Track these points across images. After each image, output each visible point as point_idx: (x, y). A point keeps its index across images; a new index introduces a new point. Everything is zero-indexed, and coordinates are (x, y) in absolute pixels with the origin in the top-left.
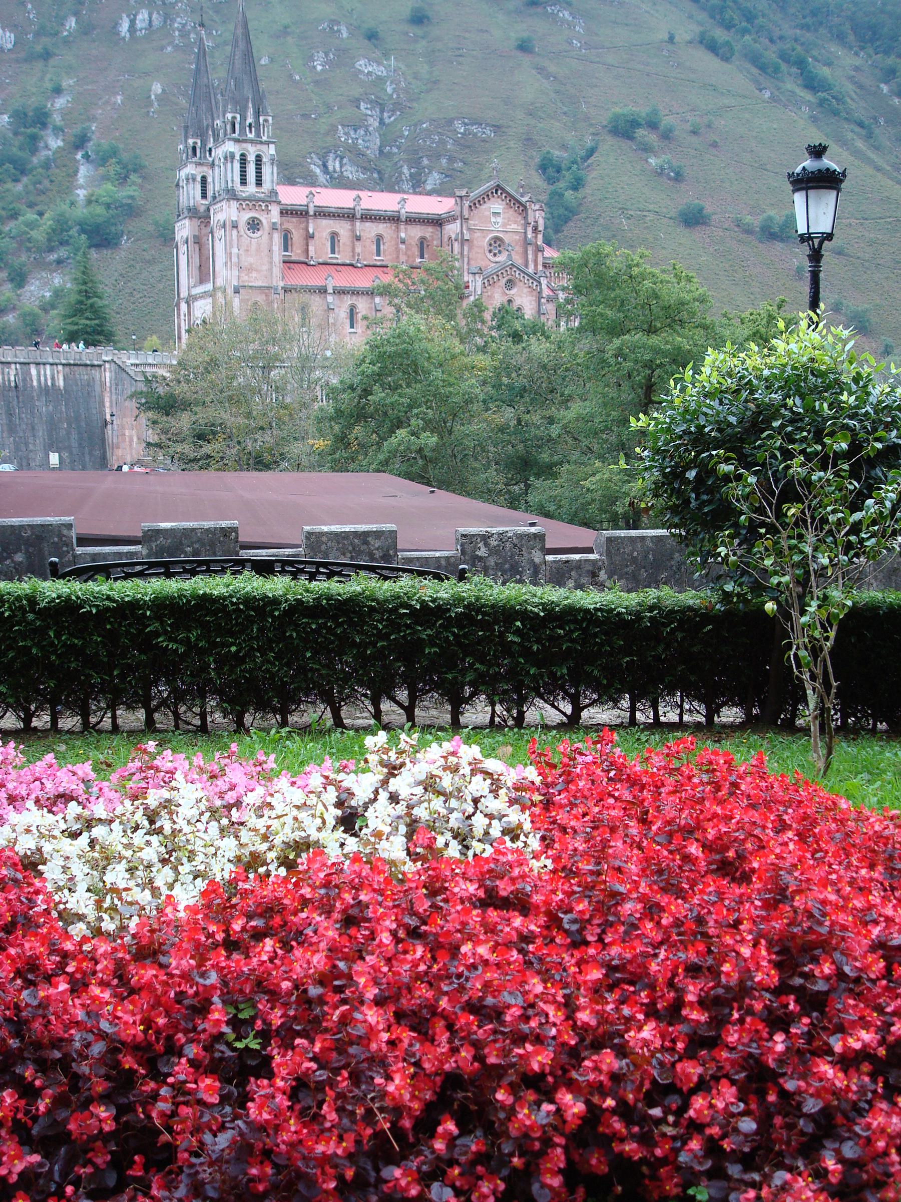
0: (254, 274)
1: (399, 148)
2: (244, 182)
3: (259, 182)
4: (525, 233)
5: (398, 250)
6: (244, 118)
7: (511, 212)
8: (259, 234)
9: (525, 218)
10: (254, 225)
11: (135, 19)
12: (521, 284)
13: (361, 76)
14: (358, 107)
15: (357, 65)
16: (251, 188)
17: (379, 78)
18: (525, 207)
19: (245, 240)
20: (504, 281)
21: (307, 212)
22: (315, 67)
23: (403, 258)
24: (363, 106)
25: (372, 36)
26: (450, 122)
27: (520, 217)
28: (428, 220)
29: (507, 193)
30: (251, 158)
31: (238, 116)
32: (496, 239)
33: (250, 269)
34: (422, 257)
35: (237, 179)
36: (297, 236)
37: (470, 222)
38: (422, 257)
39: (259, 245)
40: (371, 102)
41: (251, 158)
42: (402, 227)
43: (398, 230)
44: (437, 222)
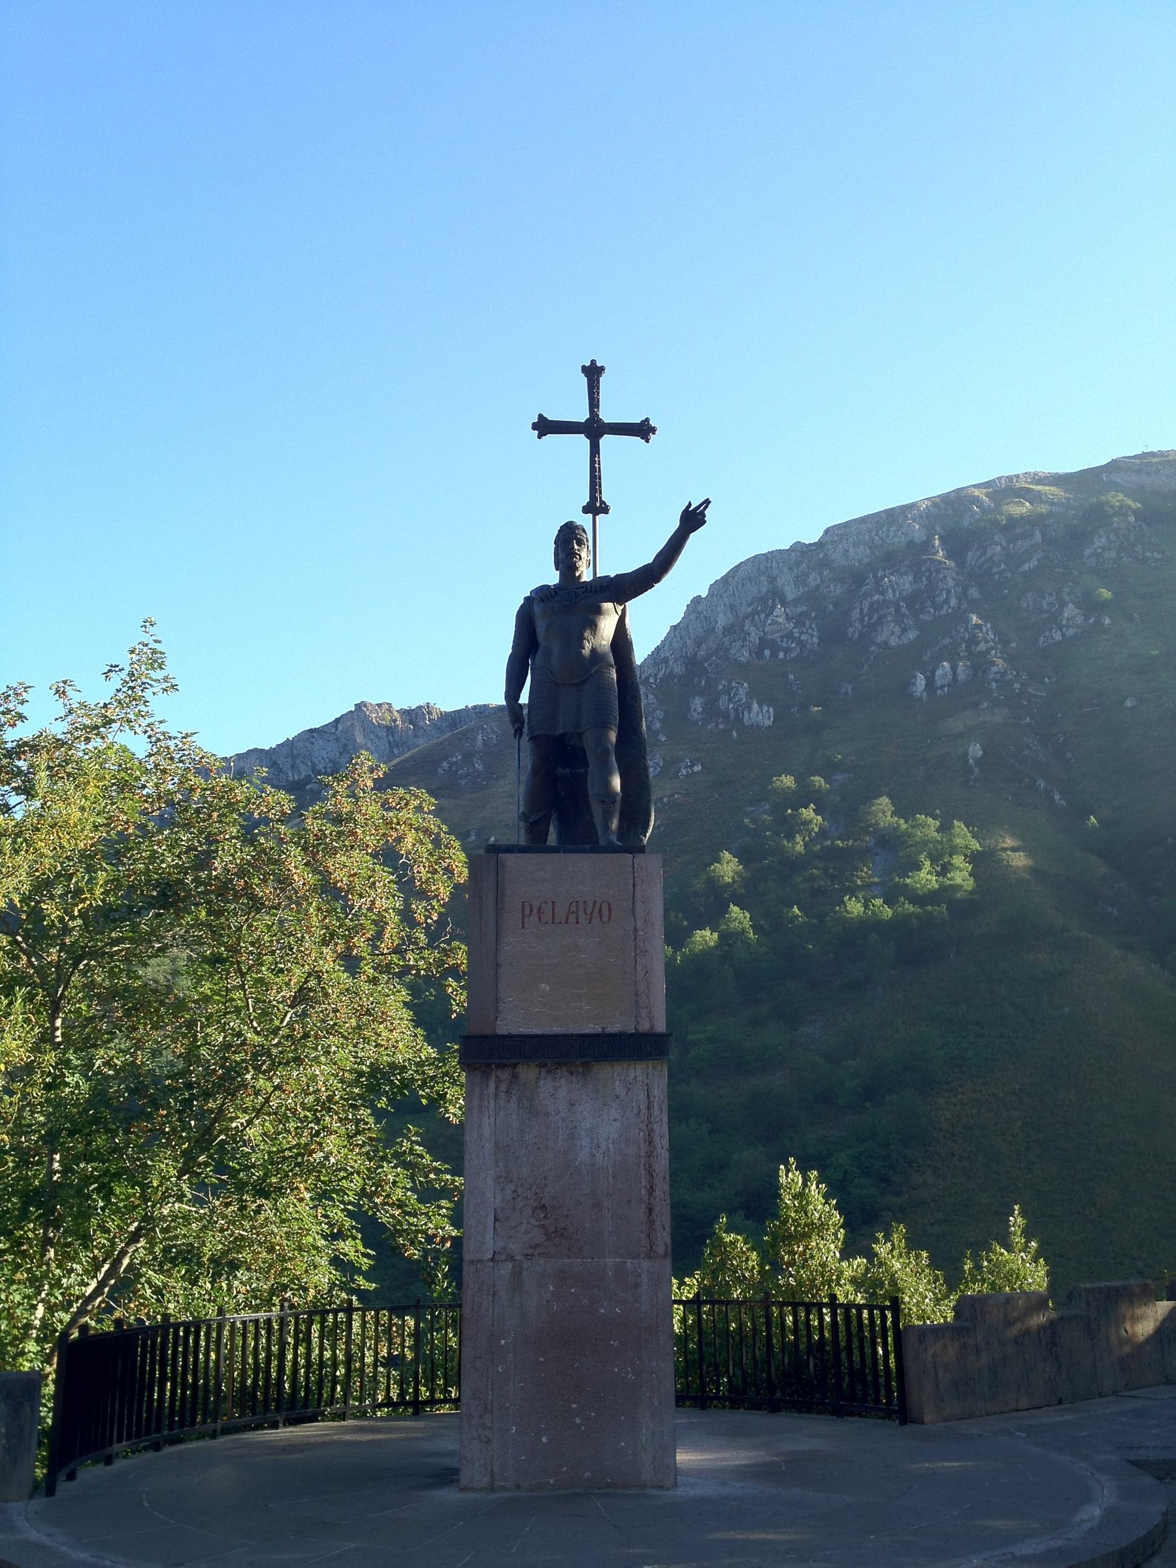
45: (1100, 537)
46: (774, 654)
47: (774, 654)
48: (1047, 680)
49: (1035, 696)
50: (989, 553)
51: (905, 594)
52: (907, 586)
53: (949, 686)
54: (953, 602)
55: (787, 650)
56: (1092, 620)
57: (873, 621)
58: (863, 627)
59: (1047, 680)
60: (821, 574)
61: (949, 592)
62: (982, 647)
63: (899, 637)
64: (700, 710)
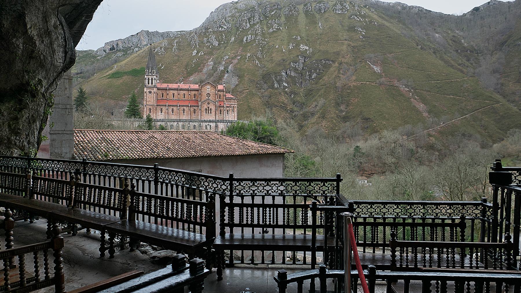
0: (150, 102)
2: (149, 84)
3: (152, 84)
6: (149, 71)
10: (150, 92)
14: (298, 57)
16: (150, 85)
19: (148, 96)
23: (190, 98)
26: (321, 60)
30: (150, 79)
33: (149, 101)
35: (147, 83)
36: (165, 94)
39: (151, 96)
41: (150, 79)
56: (279, 28)
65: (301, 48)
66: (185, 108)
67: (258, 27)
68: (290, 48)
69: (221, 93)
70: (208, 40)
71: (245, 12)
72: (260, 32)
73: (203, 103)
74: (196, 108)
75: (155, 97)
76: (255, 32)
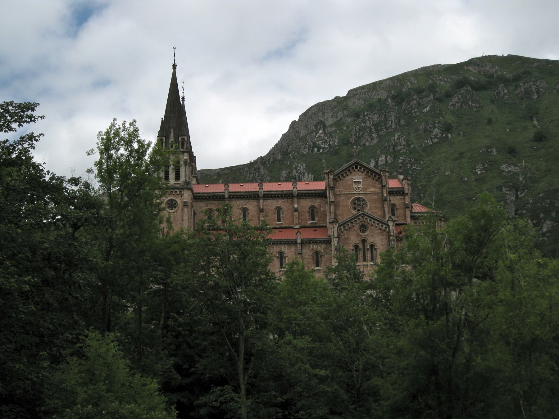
1: (526, 210)
3: (177, 178)
4: (382, 193)
5: (293, 216)
7: (370, 180)
8: (175, 209)
9: (381, 183)
11: (378, 161)
12: (373, 227)
13: (504, 174)
14: (501, 190)
15: (501, 168)
16: (172, 182)
17: (516, 174)
18: (380, 175)
20: (357, 227)
21: (224, 196)
22: (476, 172)
23: (296, 221)
24: (504, 190)
25: (512, 151)
27: (377, 183)
28: (315, 194)
29: (364, 167)
31: (164, 139)
32: (358, 199)
34: (313, 219)
37: (336, 189)
38: (313, 219)
40: (509, 187)
42: (296, 200)
43: (293, 203)
44: (322, 195)
45: (455, 97)
46: (319, 150)
47: (319, 150)
48: (422, 162)
49: (415, 169)
50: (411, 104)
51: (375, 123)
52: (376, 119)
53: (384, 165)
54: (394, 126)
55: (324, 148)
56: (444, 135)
57: (360, 135)
58: (356, 137)
59: (422, 162)
60: (343, 112)
61: (392, 122)
62: (399, 148)
63: (370, 142)
64: (285, 176)
65: (505, 171)
66: (285, 249)
67: (398, 138)
68: (479, 172)
69: (396, 200)
70: (290, 173)
71: (366, 113)
72: (403, 148)
73: (344, 226)
74: (320, 248)
75: (186, 218)
76: (394, 149)
